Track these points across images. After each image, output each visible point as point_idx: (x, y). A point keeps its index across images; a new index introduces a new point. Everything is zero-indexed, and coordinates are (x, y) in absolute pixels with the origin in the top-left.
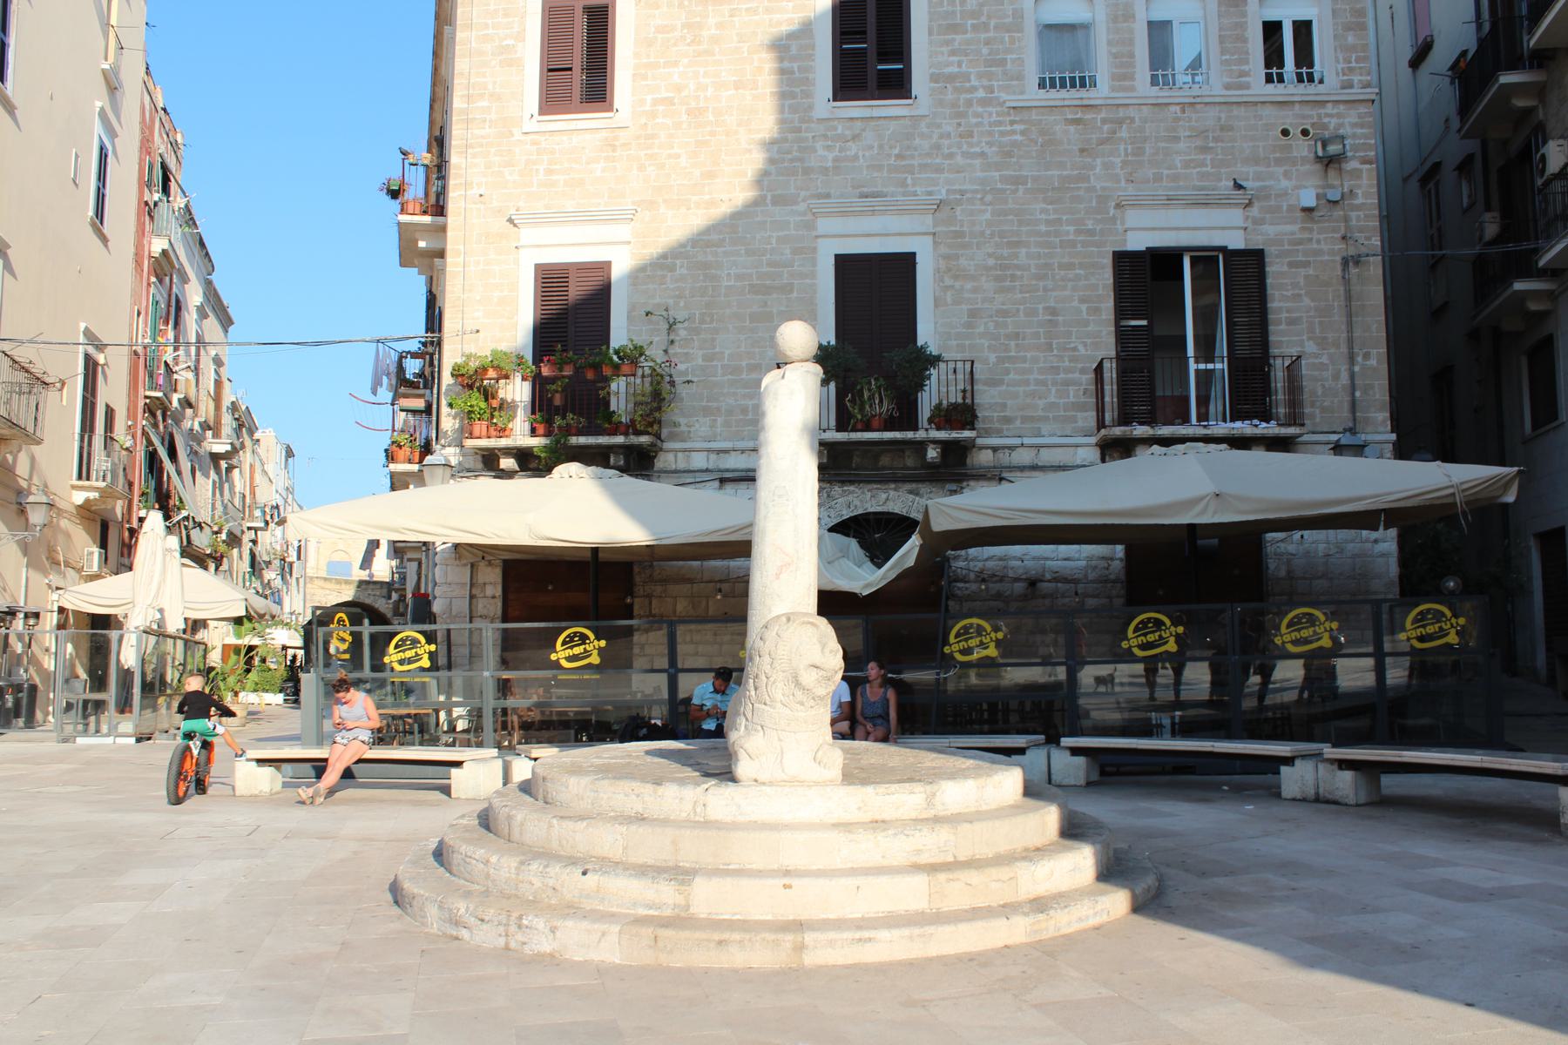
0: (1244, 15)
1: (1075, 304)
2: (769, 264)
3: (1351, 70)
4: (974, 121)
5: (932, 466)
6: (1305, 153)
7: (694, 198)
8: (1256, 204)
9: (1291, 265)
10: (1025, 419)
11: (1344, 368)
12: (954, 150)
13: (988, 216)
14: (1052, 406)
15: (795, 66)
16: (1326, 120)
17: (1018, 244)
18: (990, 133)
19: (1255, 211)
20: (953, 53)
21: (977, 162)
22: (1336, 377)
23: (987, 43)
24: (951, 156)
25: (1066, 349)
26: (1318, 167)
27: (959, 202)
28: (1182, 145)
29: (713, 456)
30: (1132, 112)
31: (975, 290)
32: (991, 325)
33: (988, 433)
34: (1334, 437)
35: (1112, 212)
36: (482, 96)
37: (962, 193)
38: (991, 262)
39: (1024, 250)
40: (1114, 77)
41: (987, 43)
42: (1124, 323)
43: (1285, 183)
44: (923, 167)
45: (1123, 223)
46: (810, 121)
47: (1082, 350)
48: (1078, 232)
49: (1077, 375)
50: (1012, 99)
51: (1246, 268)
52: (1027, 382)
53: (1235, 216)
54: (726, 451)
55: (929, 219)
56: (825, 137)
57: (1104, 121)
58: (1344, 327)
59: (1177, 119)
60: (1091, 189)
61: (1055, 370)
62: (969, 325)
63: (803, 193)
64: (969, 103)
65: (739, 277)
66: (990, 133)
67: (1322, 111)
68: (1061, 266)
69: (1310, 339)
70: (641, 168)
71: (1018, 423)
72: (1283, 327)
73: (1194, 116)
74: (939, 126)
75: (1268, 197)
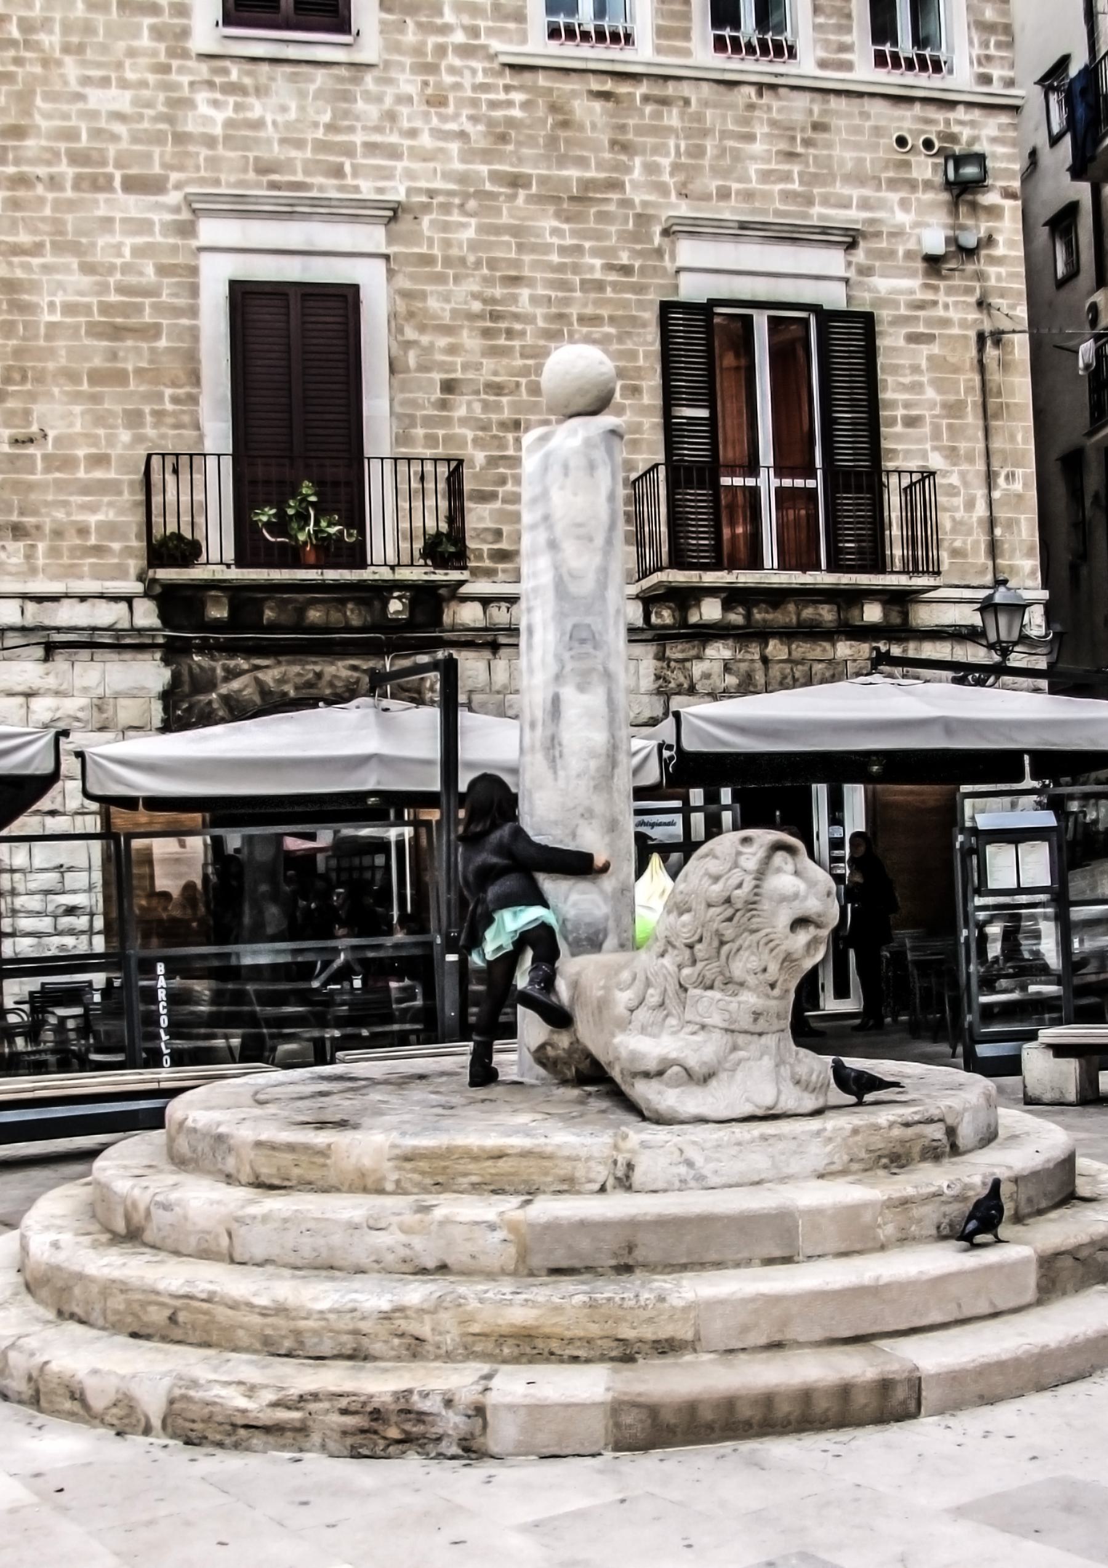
2: (121, 289)
3: (988, 58)
4: (448, 79)
5: (396, 626)
6: (928, 174)
8: (862, 244)
11: (980, 493)
12: (418, 124)
16: (955, 129)
17: (515, 280)
18: (475, 103)
19: (860, 256)
21: (454, 147)
22: (970, 505)
24: (413, 133)
26: (945, 196)
27: (426, 208)
28: (758, 147)
29: (31, 607)
30: (686, 89)
31: (452, 350)
32: (477, 407)
34: (982, 594)
35: (657, 240)
37: (431, 193)
38: (477, 306)
40: (661, 32)
44: (372, 148)
45: (673, 258)
46: (185, 54)
48: (609, 267)
50: (504, 48)
51: (853, 336)
53: (833, 261)
54: (55, 599)
56: (211, 84)
58: (980, 434)
59: (751, 107)
60: (626, 203)
62: (443, 405)
63: (174, 177)
64: (441, 50)
65: (70, 309)
66: (475, 103)
68: (582, 319)
69: (935, 448)
72: (899, 428)
73: (776, 104)
75: (878, 235)
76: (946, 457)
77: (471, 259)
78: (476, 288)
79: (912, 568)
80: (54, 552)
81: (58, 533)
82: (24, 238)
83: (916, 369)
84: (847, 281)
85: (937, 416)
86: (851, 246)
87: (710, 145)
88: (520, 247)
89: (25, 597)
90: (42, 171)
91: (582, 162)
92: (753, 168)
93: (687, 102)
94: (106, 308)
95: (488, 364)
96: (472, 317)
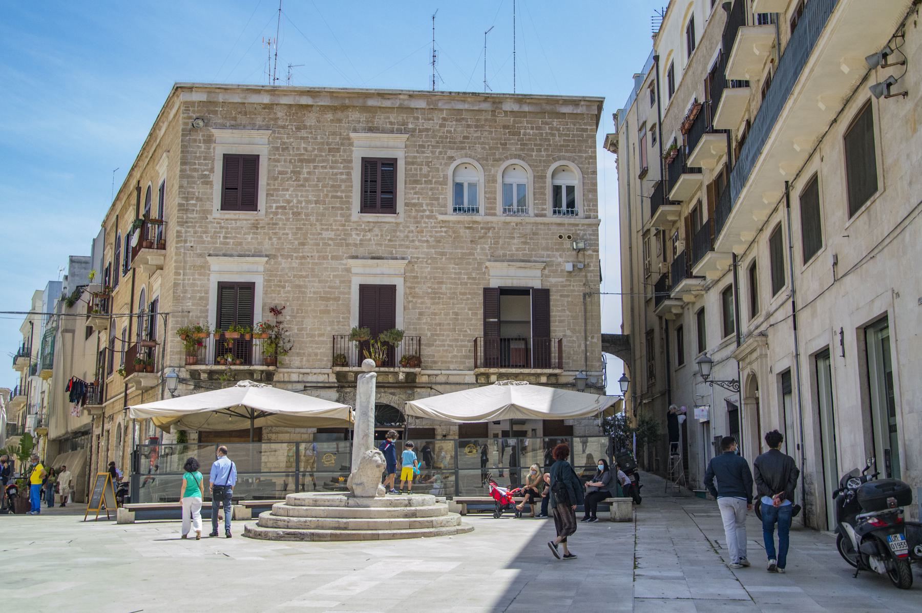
0: (545, 183)
3: (590, 210)
7: (295, 255)
9: (561, 296)
10: (443, 362)
14: (455, 356)
15: (344, 195)
17: (442, 283)
18: (431, 232)
19: (546, 272)
20: (415, 193)
22: (579, 346)
23: (431, 189)
24: (413, 241)
27: (416, 263)
28: (516, 241)
31: (422, 303)
33: (426, 368)
36: (192, 198)
37: (418, 258)
38: (430, 290)
40: (486, 208)
41: (431, 189)
43: (560, 260)
44: (401, 245)
46: (350, 221)
48: (469, 278)
51: (542, 297)
52: (444, 346)
57: (482, 228)
61: (457, 340)
64: (422, 217)
65: (314, 293)
66: (431, 232)
68: (461, 294)
70: (270, 239)
74: (408, 227)
75: (552, 266)
79: (560, 366)
80: (308, 361)
81: (309, 355)
82: (304, 273)
83: (563, 305)
87: (501, 242)
89: (300, 373)
90: (309, 254)
91: (462, 248)
94: (325, 293)
95: (433, 307)
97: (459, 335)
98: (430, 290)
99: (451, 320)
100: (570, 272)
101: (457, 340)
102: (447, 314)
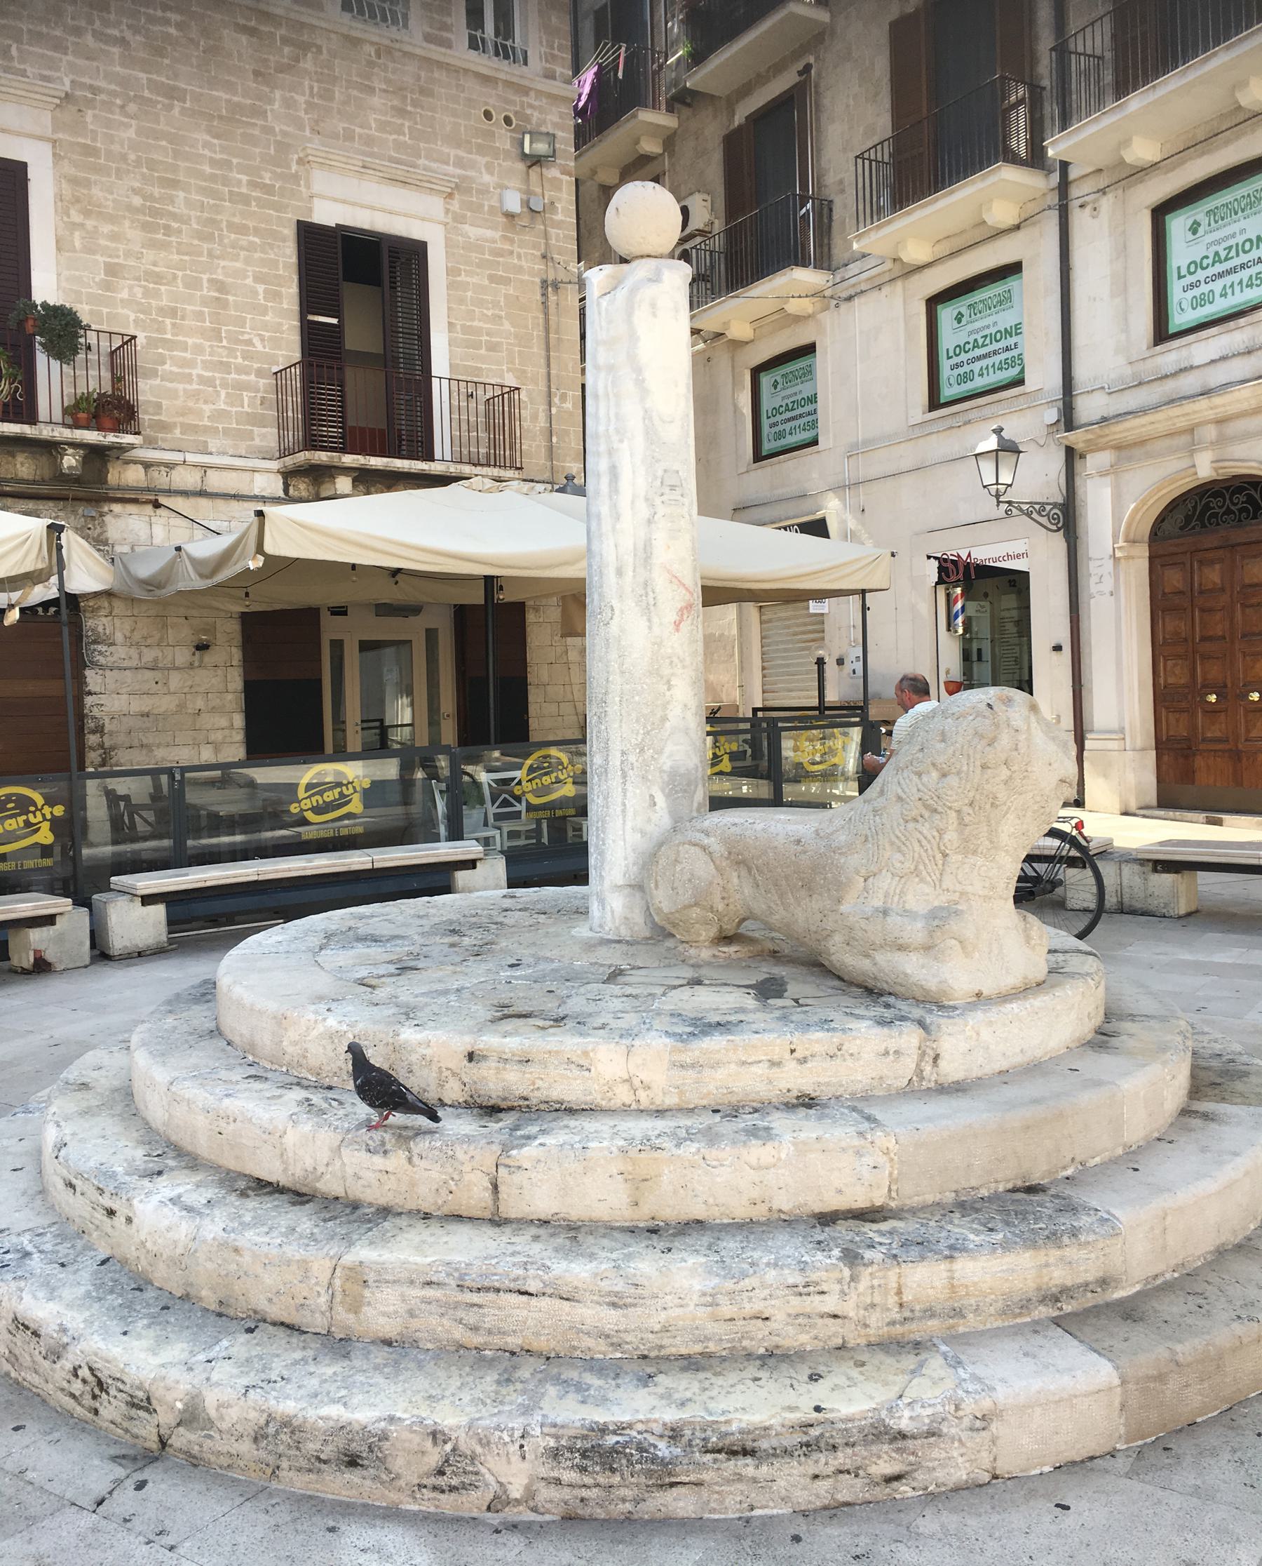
1: (249, 281)
3: (553, 56)
10: (186, 428)
11: (543, 408)
13: (131, 133)
14: (220, 415)
16: (529, 112)
17: (174, 184)
19: (455, 205)
25: (238, 341)
26: (521, 166)
27: (90, 103)
32: (139, 292)
33: (151, 443)
35: (294, 167)
38: (137, 201)
39: (181, 194)
42: (311, 317)
43: (487, 178)
45: (308, 187)
47: (260, 347)
49: (252, 377)
52: (188, 378)
55: (46, 118)
58: (543, 361)
59: (371, 64)
60: (268, 130)
61: (225, 367)
62: (107, 286)
67: (525, 99)
68: (232, 227)
69: (509, 370)
71: (177, 431)
76: (517, 378)
77: (132, 157)
78: (137, 185)
84: (446, 224)
85: (511, 344)
86: (450, 195)
88: (176, 155)
92: (372, 118)
93: (319, 48)
95: (150, 255)
96: (130, 208)
97: (231, 352)
98: (137, 201)
99: (205, 302)
100: (510, 216)
101: (225, 367)
102: (194, 284)
